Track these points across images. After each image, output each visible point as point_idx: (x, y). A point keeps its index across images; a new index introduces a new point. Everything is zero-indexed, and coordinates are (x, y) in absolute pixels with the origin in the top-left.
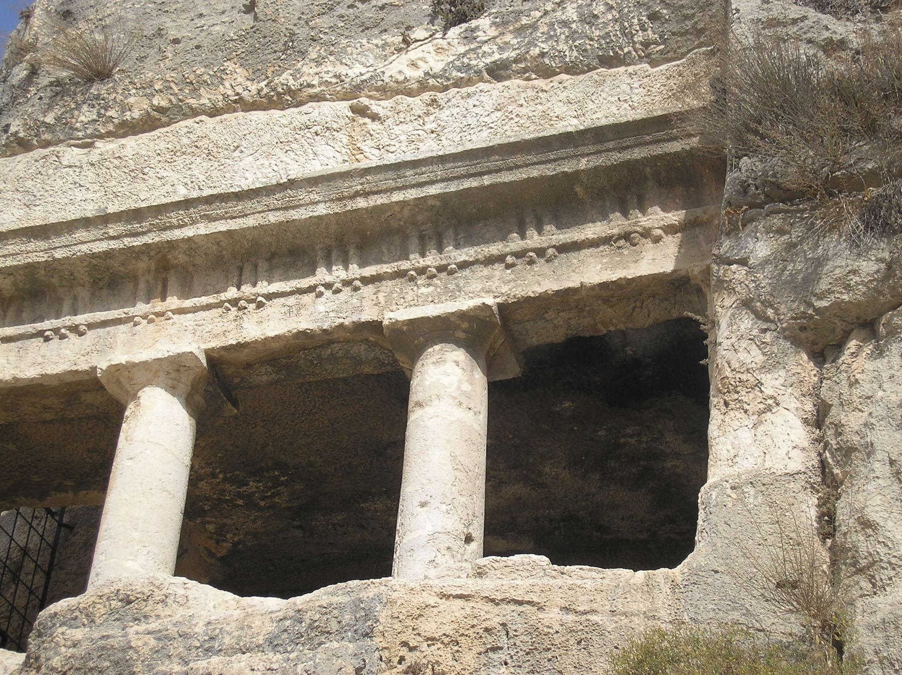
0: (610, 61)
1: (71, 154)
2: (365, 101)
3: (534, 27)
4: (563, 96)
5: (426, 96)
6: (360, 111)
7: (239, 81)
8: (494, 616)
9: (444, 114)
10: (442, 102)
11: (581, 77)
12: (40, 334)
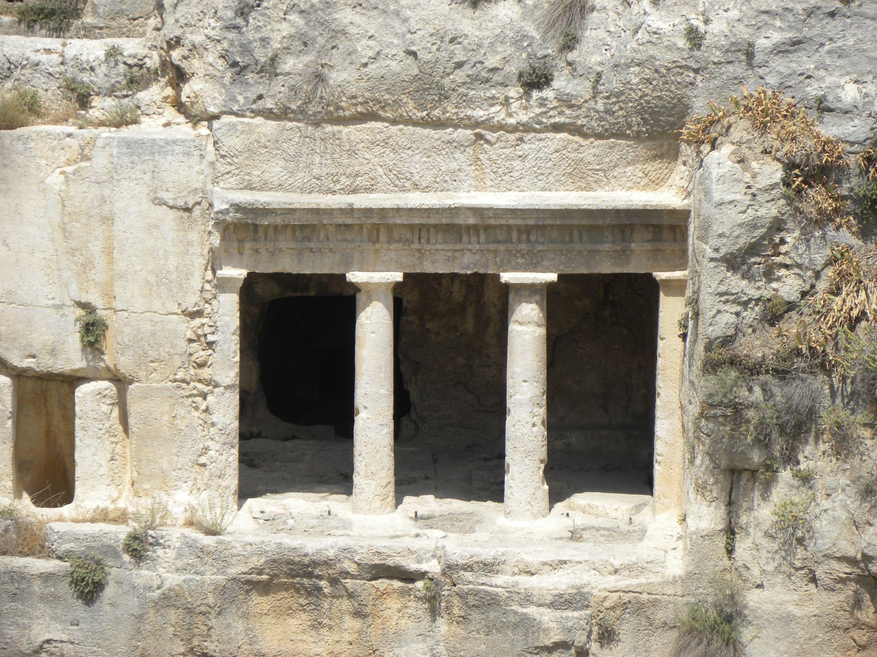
0: (620, 135)
2: (483, 132)
3: (580, 107)
4: (592, 151)
5: (518, 135)
6: (479, 136)
7: (410, 108)
8: (626, 598)
9: (526, 146)
10: (526, 140)
11: (602, 142)
12: (311, 249)
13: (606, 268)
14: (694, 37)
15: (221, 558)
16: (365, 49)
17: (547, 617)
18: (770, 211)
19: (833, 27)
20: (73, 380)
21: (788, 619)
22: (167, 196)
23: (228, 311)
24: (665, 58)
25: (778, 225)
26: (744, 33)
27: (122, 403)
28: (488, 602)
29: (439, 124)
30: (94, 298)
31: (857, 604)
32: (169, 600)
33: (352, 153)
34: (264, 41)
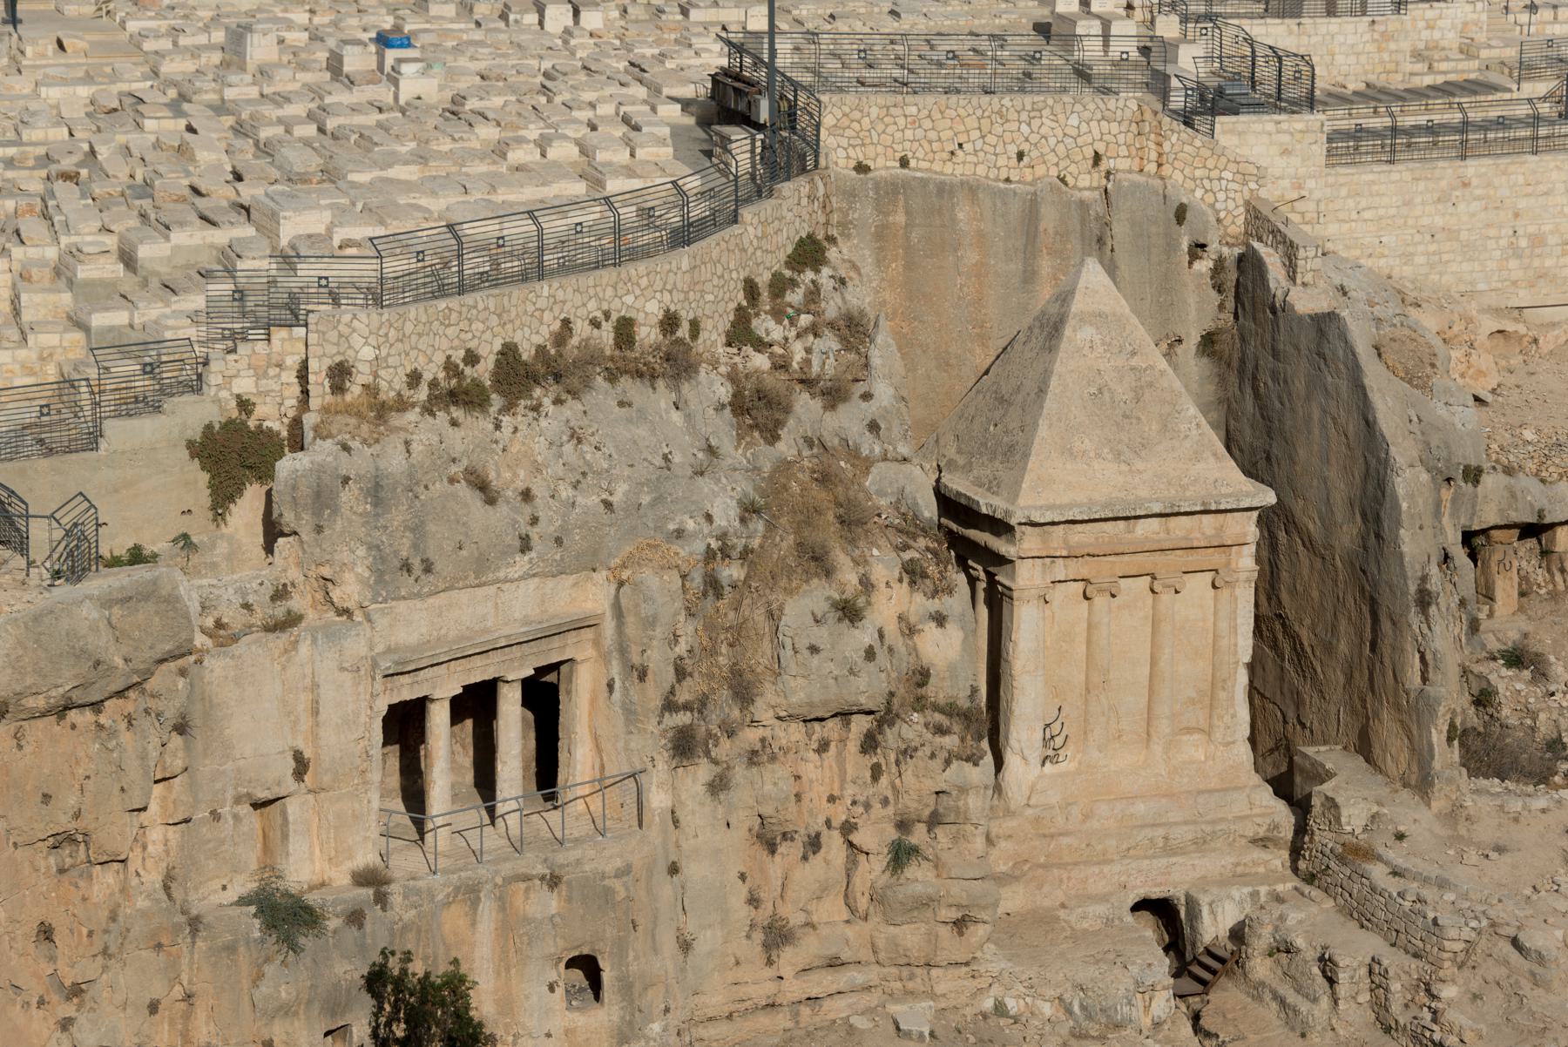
1: (418, 603)
7: (472, 580)
14: (608, 505)
17: (617, 885)
22: (346, 665)
29: (484, 584)
30: (300, 744)
33: (440, 615)
34: (396, 553)
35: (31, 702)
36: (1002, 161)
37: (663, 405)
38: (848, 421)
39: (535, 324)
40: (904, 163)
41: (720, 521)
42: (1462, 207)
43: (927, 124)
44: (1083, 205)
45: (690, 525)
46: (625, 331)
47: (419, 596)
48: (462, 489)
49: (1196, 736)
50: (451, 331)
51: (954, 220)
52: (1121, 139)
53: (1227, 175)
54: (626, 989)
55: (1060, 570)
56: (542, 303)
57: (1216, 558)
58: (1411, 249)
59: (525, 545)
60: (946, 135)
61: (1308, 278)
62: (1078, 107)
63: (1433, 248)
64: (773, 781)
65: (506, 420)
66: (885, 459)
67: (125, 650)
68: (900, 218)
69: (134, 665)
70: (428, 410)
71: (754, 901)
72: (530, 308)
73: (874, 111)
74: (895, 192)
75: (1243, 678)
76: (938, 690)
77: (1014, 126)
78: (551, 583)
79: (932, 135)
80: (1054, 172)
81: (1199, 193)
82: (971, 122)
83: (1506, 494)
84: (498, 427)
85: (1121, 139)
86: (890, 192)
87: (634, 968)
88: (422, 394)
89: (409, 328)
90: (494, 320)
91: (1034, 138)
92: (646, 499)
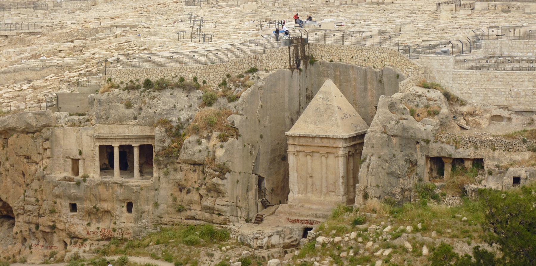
7: (119, 122)
13: (146, 143)
14: (155, 112)
15: (94, 181)
16: (113, 115)
17: (134, 188)
18: (163, 135)
19: (172, 111)
20: (78, 160)
21: (166, 188)
23: (97, 150)
24: (151, 115)
25: (164, 136)
26: (161, 112)
27: (84, 163)
28: (127, 186)
31: (174, 185)
32: (88, 187)
35: (18, 130)
36: (361, 61)
37: (183, 95)
38: (232, 105)
39: (157, 76)
40: (340, 60)
41: (182, 120)
42: (496, 83)
43: (346, 51)
44: (376, 72)
45: (174, 119)
46: (182, 80)
47: (105, 124)
48: (122, 105)
49: (333, 193)
50: (134, 75)
51: (349, 74)
52: (387, 57)
53: (411, 68)
54: (137, 211)
55: (298, 148)
56: (158, 72)
57: (333, 150)
58: (479, 92)
59: (135, 118)
60: (349, 54)
61: (402, 90)
62: (378, 49)
63: (486, 92)
64: (179, 176)
65: (142, 93)
66: (237, 113)
67: (37, 123)
68: (338, 73)
69: (38, 126)
70: (123, 90)
71: (175, 200)
72: (155, 72)
73: (335, 48)
74: (337, 67)
75: (341, 180)
76: (217, 162)
77: (364, 53)
78: (143, 128)
79: (347, 54)
80: (372, 64)
81: (405, 71)
82: (355, 52)
83: (440, 149)
84: (141, 95)
85: (387, 57)
86: (336, 66)
87: (140, 207)
88: (123, 86)
89: (122, 73)
90: (145, 74)
91: (368, 56)
92: (164, 113)
